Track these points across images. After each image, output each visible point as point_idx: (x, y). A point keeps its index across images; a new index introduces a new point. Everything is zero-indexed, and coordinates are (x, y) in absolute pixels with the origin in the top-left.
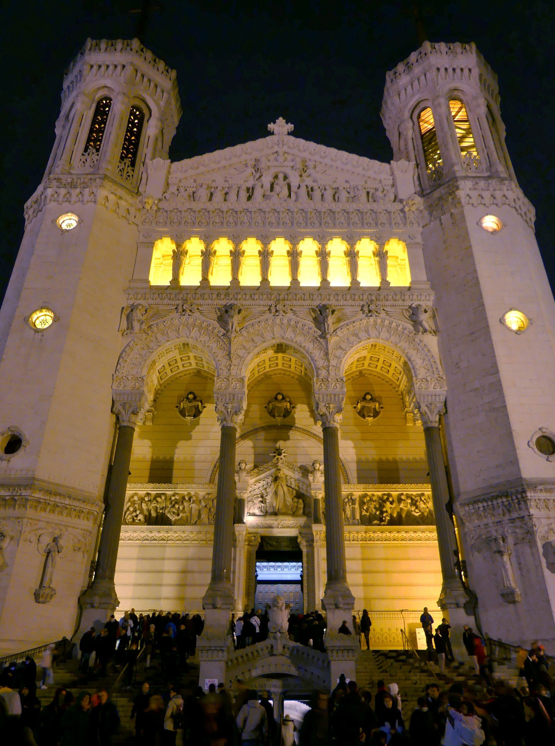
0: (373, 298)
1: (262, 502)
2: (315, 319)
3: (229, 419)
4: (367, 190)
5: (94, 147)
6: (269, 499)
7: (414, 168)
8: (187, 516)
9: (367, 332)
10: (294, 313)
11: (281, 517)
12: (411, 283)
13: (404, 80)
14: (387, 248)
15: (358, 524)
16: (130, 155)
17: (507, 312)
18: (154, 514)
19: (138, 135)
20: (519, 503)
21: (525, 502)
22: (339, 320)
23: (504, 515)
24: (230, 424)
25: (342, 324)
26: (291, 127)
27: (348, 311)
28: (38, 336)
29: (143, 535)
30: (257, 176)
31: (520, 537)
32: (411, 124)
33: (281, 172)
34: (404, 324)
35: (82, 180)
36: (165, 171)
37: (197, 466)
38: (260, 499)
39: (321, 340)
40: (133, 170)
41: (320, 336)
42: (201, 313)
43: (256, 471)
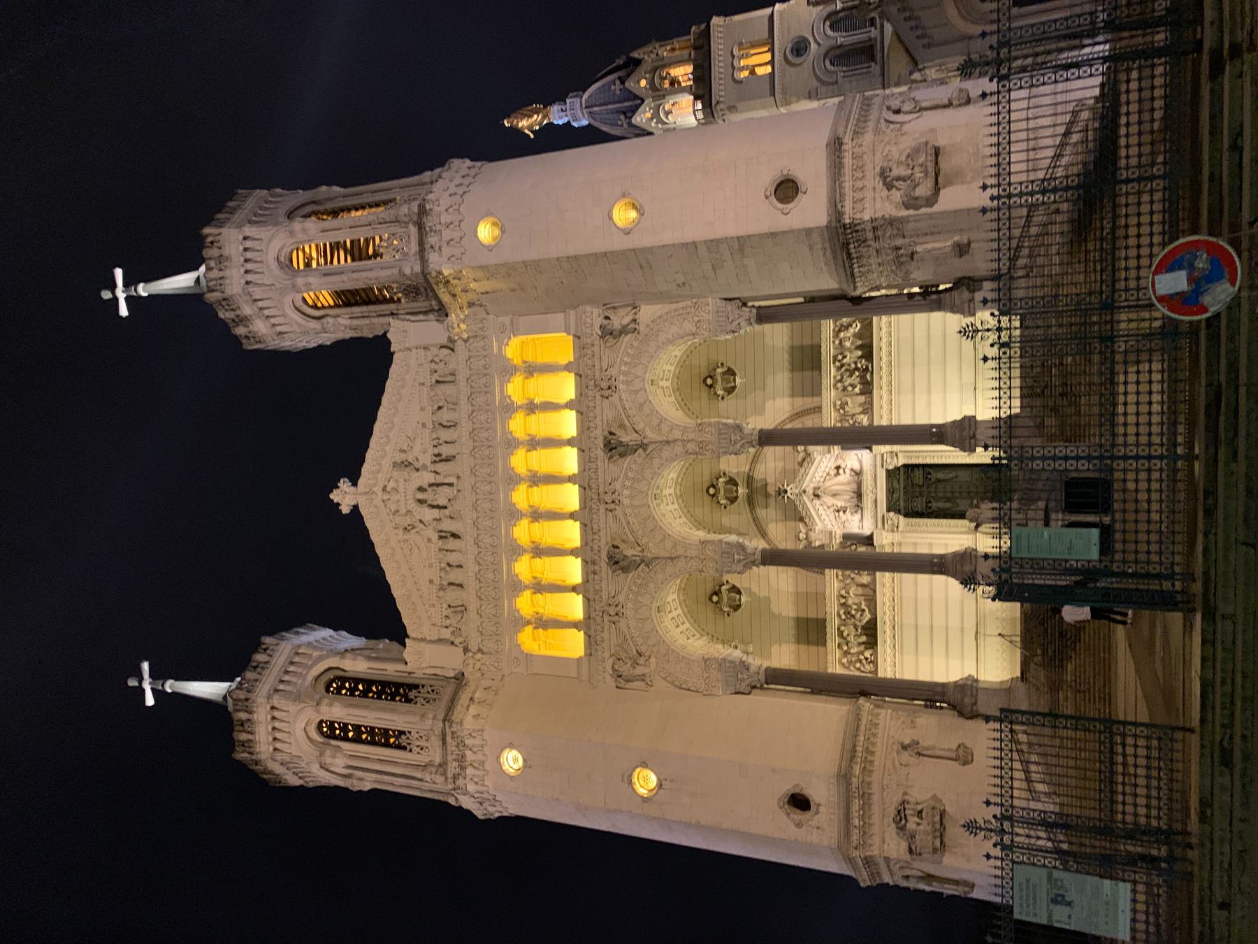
0: (592, 383)
1: (844, 512)
2: (622, 455)
3: (752, 558)
4: (433, 381)
5: (397, 737)
6: (840, 504)
7: (398, 319)
8: (865, 600)
9: (636, 392)
10: (614, 480)
11: (864, 489)
12: (569, 334)
13: (260, 327)
14: (517, 361)
15: (872, 400)
16: (401, 691)
17: (615, 225)
18: (864, 639)
19: (369, 683)
20: (857, 231)
21: (855, 225)
22: (622, 426)
23: (869, 246)
24: (758, 556)
25: (626, 422)
26: (344, 484)
27: (609, 414)
28: (666, 784)
29: (888, 650)
30: (422, 526)
31: (895, 232)
32: (330, 320)
33: (414, 495)
34: (624, 344)
35: (454, 748)
36: (422, 644)
37: (802, 589)
38: (841, 513)
39: (650, 449)
40: (423, 686)
41: (645, 450)
42: (620, 592)
43: (807, 520)
